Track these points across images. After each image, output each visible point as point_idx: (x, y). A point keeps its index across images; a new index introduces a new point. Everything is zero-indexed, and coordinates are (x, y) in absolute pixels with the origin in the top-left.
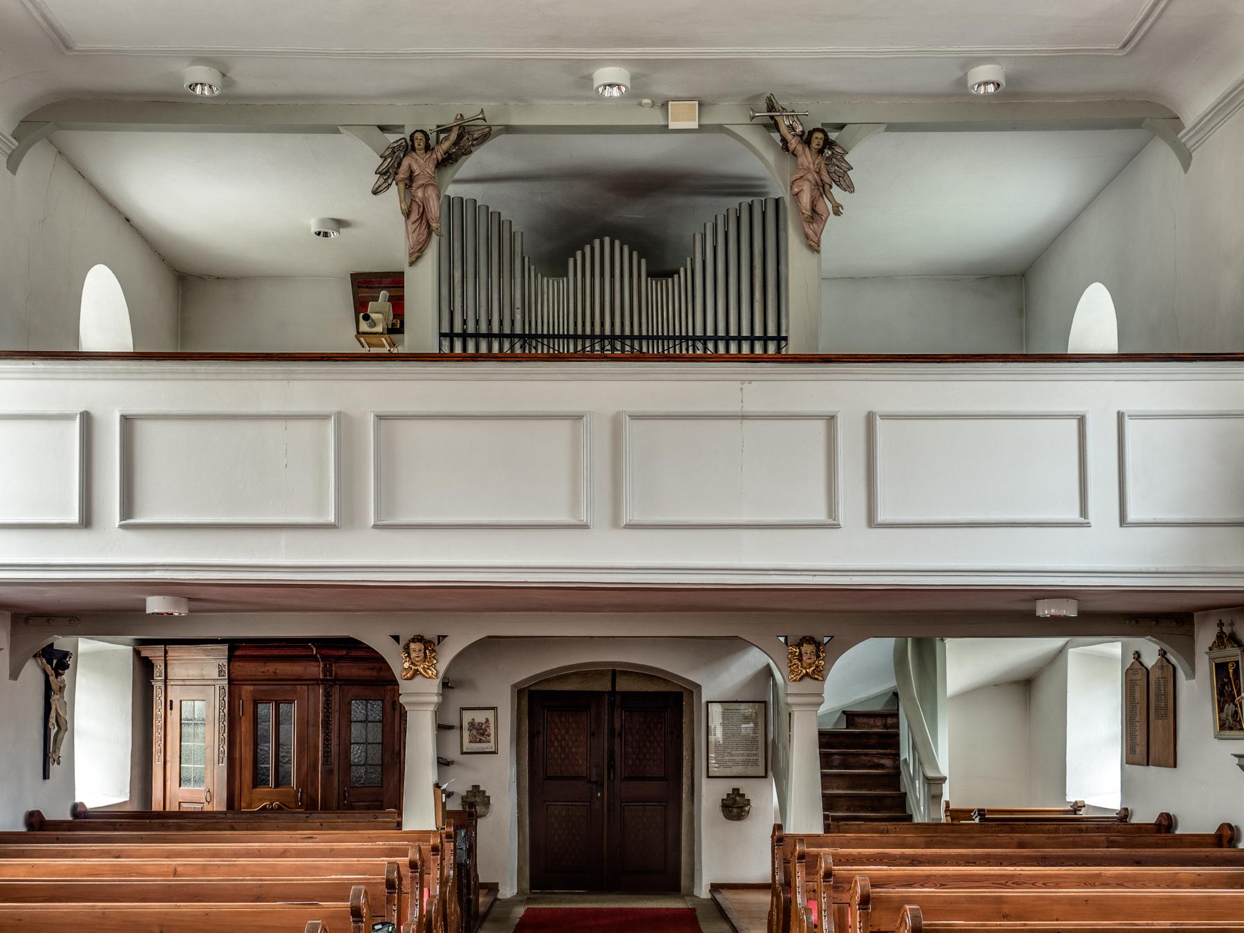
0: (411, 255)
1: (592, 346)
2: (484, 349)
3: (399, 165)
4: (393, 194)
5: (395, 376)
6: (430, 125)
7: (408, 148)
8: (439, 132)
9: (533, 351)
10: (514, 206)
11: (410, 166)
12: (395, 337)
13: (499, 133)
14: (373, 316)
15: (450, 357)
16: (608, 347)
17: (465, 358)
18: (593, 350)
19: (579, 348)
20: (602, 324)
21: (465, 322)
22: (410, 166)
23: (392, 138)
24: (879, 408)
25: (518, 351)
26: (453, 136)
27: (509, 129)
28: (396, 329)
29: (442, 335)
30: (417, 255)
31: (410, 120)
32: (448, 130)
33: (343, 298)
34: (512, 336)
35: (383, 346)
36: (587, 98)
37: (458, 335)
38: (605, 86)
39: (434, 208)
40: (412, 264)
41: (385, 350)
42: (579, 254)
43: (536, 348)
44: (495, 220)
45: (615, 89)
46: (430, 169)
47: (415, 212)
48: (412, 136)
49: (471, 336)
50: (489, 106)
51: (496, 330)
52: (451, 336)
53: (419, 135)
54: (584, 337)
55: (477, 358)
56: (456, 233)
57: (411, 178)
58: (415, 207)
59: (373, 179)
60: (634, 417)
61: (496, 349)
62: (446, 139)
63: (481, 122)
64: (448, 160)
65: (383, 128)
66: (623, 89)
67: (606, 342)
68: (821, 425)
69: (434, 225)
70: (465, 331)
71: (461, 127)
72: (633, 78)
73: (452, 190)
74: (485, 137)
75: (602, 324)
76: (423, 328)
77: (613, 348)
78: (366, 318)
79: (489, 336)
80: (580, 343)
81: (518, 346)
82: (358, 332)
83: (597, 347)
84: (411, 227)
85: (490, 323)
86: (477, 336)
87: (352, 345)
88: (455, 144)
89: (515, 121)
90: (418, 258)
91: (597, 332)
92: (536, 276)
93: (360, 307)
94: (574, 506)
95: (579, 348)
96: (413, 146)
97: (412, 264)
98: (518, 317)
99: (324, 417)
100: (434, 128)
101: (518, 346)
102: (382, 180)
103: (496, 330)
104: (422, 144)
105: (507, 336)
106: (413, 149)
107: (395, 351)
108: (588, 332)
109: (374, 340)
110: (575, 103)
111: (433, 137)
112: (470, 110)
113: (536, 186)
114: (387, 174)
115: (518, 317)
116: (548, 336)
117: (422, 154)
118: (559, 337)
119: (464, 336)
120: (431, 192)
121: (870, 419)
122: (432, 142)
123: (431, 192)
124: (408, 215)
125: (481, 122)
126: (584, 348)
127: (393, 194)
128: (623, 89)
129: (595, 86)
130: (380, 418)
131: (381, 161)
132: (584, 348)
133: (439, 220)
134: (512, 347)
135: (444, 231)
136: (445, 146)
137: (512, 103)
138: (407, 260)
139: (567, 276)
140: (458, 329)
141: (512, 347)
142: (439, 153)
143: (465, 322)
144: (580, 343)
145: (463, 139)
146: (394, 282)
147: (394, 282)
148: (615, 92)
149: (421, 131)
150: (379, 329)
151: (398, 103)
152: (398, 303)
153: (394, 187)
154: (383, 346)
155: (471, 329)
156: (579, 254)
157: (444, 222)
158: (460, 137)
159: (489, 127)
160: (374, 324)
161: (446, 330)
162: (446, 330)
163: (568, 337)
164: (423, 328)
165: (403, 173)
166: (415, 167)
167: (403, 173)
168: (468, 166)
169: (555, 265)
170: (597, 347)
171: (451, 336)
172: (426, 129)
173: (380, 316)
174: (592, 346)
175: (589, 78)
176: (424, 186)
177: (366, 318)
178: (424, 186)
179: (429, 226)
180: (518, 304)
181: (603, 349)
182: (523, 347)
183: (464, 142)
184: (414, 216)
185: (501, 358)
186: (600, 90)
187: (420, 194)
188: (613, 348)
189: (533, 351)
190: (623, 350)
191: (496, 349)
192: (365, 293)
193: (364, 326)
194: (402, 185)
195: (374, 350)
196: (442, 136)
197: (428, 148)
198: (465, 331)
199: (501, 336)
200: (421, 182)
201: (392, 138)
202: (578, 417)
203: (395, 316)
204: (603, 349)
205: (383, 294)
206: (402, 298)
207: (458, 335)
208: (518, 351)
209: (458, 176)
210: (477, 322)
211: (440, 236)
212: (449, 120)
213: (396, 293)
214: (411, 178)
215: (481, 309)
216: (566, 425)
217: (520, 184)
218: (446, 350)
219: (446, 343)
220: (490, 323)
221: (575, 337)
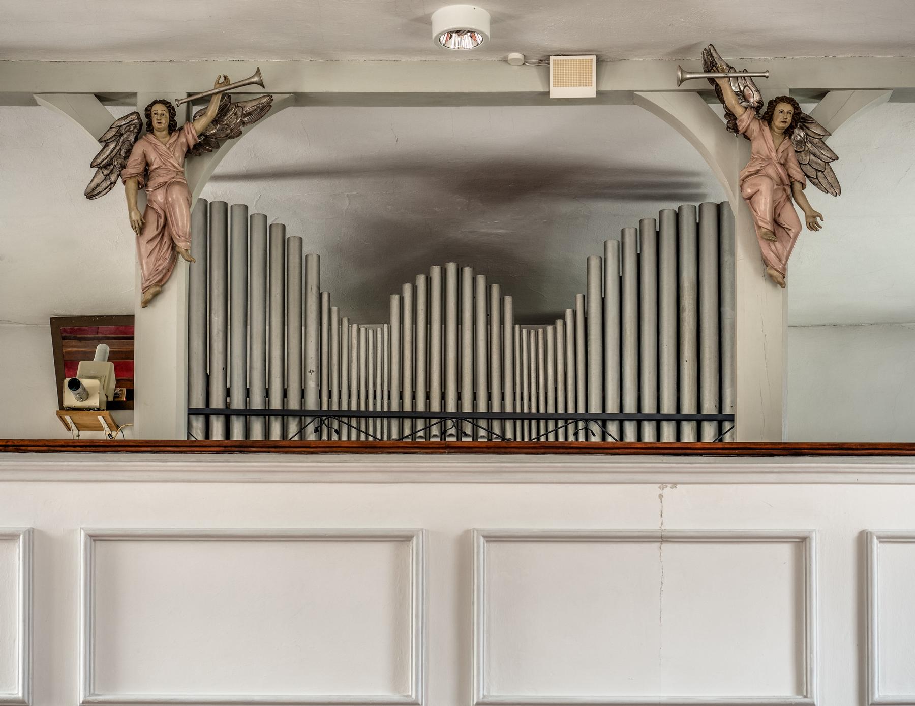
0: (145, 290)
1: (427, 428)
2: (257, 434)
3: (129, 152)
4: (119, 196)
5: (119, 476)
6: (177, 93)
7: (143, 126)
8: (191, 103)
9: (335, 437)
10: (307, 215)
11: (145, 156)
12: (120, 415)
13: (284, 104)
14: (85, 382)
15: (205, 447)
16: (452, 431)
17: (228, 447)
18: (428, 435)
19: (407, 432)
20: (443, 396)
21: (228, 392)
22: (145, 156)
23: (117, 112)
24: (876, 526)
25: (311, 437)
26: (213, 109)
27: (299, 99)
28: (121, 402)
29: (192, 412)
30: (154, 291)
31: (146, 84)
32: (205, 100)
33: (40, 353)
34: (301, 414)
35: (100, 428)
36: (421, 51)
37: (217, 413)
38: (450, 33)
39: (183, 219)
40: (146, 304)
41: (102, 435)
42: (407, 289)
43: (338, 432)
44: (281, 241)
45: (467, 37)
46: (177, 158)
47: (154, 226)
48: (148, 110)
49: (238, 413)
50: (269, 65)
51: (276, 404)
52: (207, 414)
53: (159, 109)
54: (414, 416)
55: (246, 447)
56: (209, 252)
57: (146, 173)
58: (152, 218)
59: (87, 175)
60: (493, 538)
61: (276, 435)
62: (202, 113)
63: (256, 89)
64: (204, 146)
65: (103, 98)
66: (479, 38)
67: (449, 423)
68: (785, 552)
69: (181, 245)
70: (227, 405)
71: (226, 95)
72: (494, 21)
73: (211, 192)
74: (262, 111)
75: (443, 396)
76: (162, 401)
77: (461, 433)
78: (75, 385)
79: (266, 414)
80: (407, 423)
81: (310, 429)
82: (61, 407)
83: (435, 431)
84: (146, 248)
85: (267, 393)
86: (247, 413)
87: (50, 426)
88: (215, 121)
89: (310, 86)
90: (156, 295)
91: (435, 407)
92: (340, 322)
93: (66, 369)
94: (397, 675)
95: (407, 432)
96: (150, 124)
97: (146, 304)
98: (312, 385)
99: (11, 537)
100: (183, 96)
101: (310, 429)
102: (101, 177)
103: (276, 404)
104: (165, 122)
105: (294, 414)
106: (151, 129)
107: (118, 436)
108: (421, 407)
109: (85, 418)
110: (403, 59)
111: (181, 111)
112: (239, 70)
113: (341, 185)
114: (109, 167)
115: (312, 385)
116: (359, 415)
117: (157, 139)
118: (375, 415)
119: (227, 414)
120: (177, 194)
121: (863, 542)
122: (180, 119)
123: (177, 194)
124: (140, 229)
125: (256, 89)
126: (414, 432)
127: (119, 196)
128: (479, 38)
129: (434, 35)
130: (95, 538)
131: (100, 147)
132: (414, 432)
133: (189, 237)
134: (301, 431)
135: (197, 254)
136: (200, 124)
137: (305, 60)
138: (138, 299)
139: (388, 322)
140: (217, 402)
141: (301, 431)
142: (190, 136)
143: (228, 392)
144: (407, 423)
145: (228, 114)
146: (118, 331)
147: (118, 331)
148: (467, 42)
149: (164, 102)
150: (94, 402)
151: (128, 59)
152: (124, 364)
153: (120, 187)
154: (100, 428)
155: (237, 402)
156: (407, 289)
157: (198, 240)
158: (223, 110)
159: (270, 95)
160: (86, 395)
161: (198, 402)
162: (198, 402)
163: (389, 415)
164: (162, 401)
165: (134, 165)
166: (153, 157)
167: (134, 165)
168: (234, 156)
169: (371, 305)
170: (435, 431)
171: (207, 414)
172: (171, 99)
173: (96, 382)
174: (427, 428)
175: (426, 21)
176: (167, 185)
177: (75, 385)
178: (167, 185)
179: (173, 247)
180: (312, 364)
181: (443, 433)
182: (318, 430)
183: (230, 119)
184: (151, 230)
185: (284, 447)
186: (443, 39)
187: (160, 197)
188: (461, 433)
189: (335, 437)
190: (475, 436)
191: (276, 435)
192: (72, 347)
193: (71, 399)
194: (132, 184)
195: (86, 435)
196: (195, 109)
197: (172, 128)
198: (227, 405)
199: (284, 414)
200: (161, 180)
201: (117, 112)
202: (404, 539)
203: (119, 383)
204: (443, 433)
205: (102, 350)
206: (130, 355)
207: (217, 413)
208: (311, 437)
209: (219, 170)
210: (248, 392)
211: (190, 261)
212: (205, 85)
213: (121, 347)
214: (146, 173)
215: (252, 374)
216: (383, 551)
217: (314, 182)
218: (199, 435)
219: (198, 423)
220: (267, 393)
221: (401, 416)
